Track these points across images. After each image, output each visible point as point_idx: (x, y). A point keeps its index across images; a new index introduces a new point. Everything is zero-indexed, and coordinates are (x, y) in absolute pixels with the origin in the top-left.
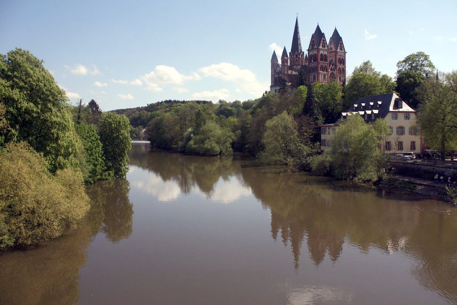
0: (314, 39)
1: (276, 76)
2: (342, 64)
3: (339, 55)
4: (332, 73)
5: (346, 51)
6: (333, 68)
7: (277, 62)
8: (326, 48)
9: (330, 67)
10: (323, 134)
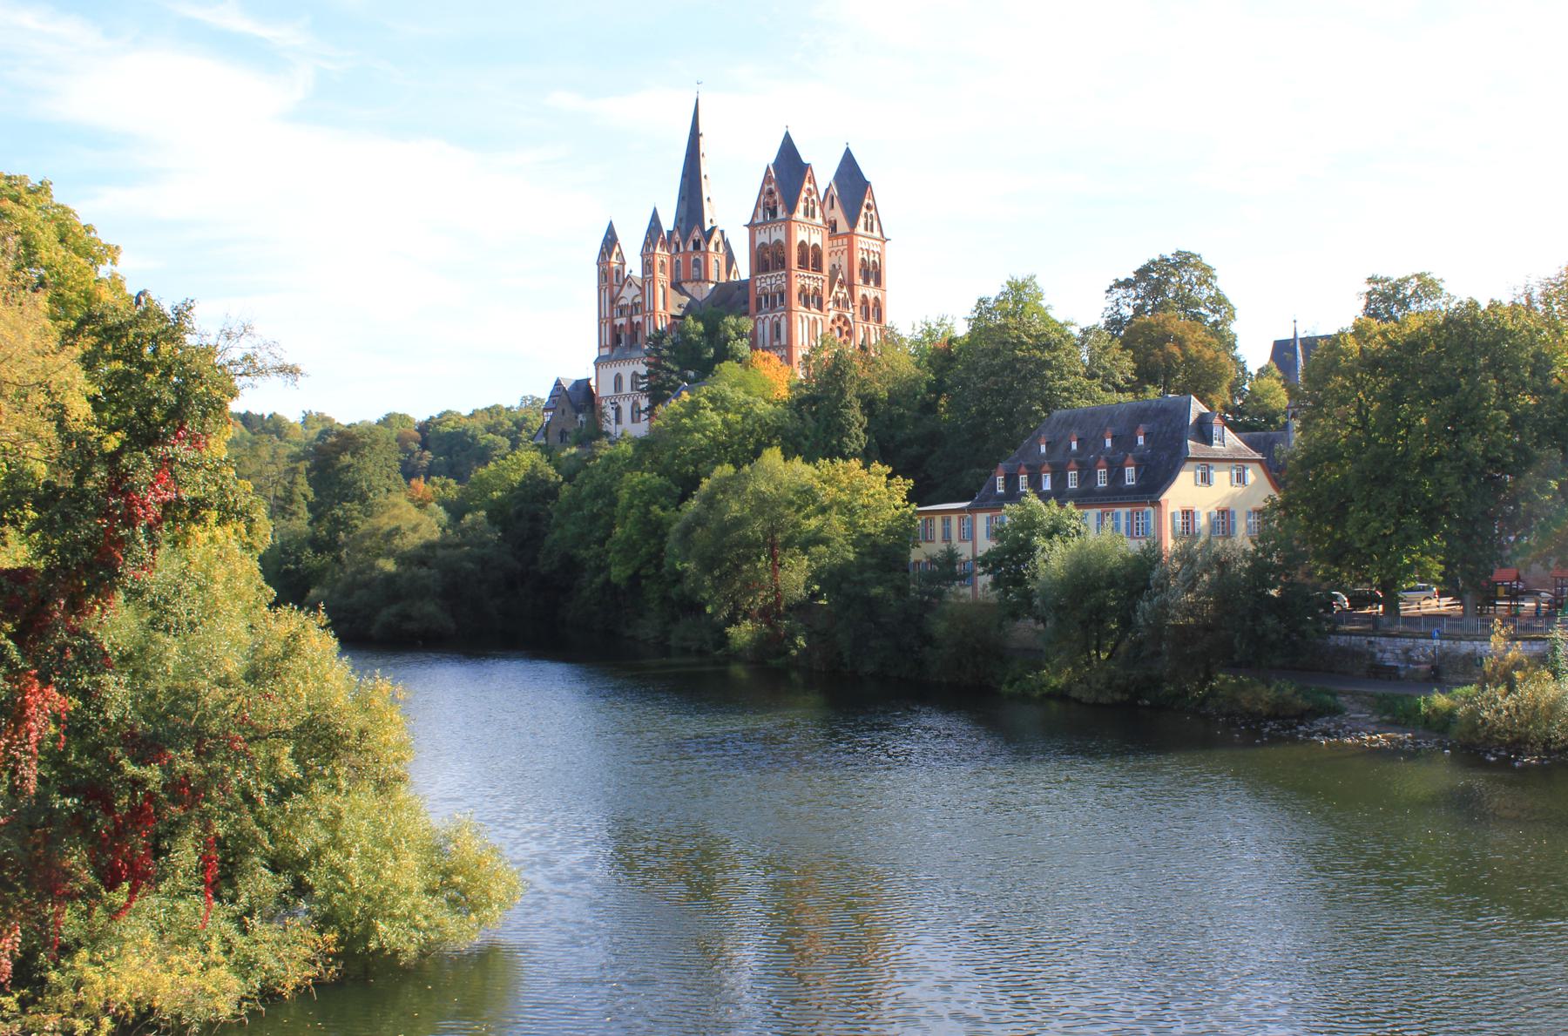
0: (773, 186)
1: (618, 322)
2: (872, 283)
4: (839, 319)
6: (841, 296)
8: (819, 220)
9: (834, 294)
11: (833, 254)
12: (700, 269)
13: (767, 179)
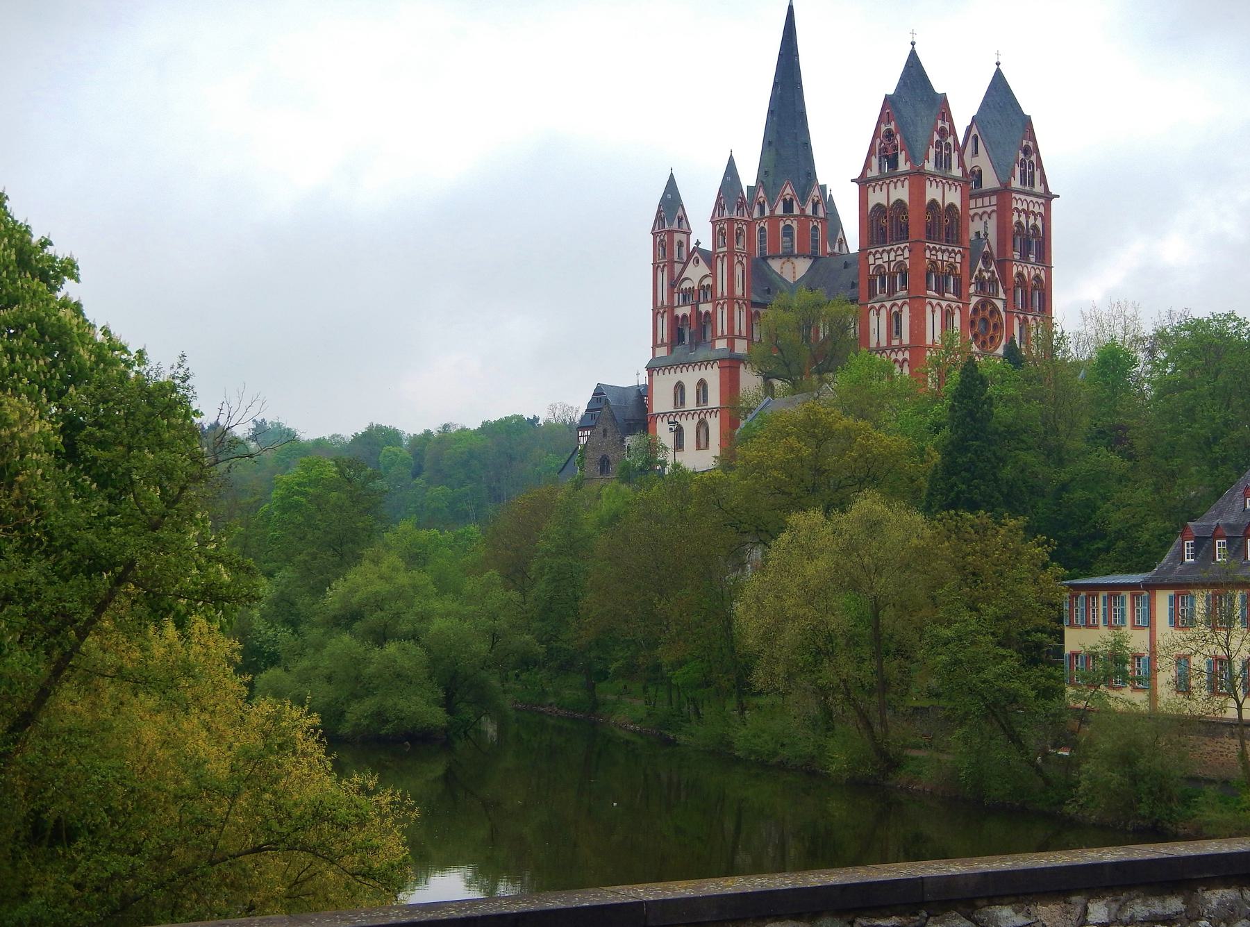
0: (892, 126)
1: (680, 312)
2: (1032, 258)
3: (1019, 211)
4: (983, 304)
7: (683, 237)
8: (956, 172)
9: (977, 272)
10: (1071, 625)
11: (977, 218)
12: (792, 240)
13: (884, 117)
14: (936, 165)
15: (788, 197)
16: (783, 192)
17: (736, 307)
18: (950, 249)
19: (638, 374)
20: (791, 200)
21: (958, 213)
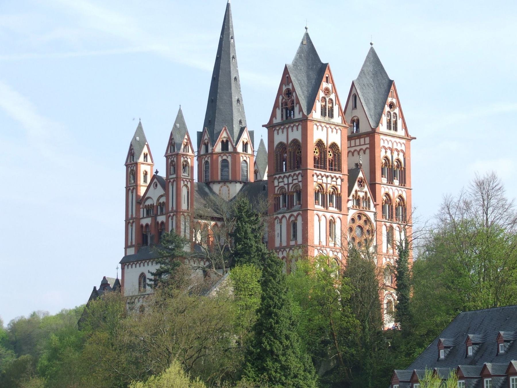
0: (290, 87)
2: (396, 182)
4: (360, 217)
5: (411, 134)
7: (148, 168)
8: (337, 119)
9: (353, 192)
14: (322, 115)
15: (225, 140)
16: (221, 135)
17: (182, 218)
18: (333, 175)
19: (117, 268)
20: (227, 141)
21: (339, 150)
